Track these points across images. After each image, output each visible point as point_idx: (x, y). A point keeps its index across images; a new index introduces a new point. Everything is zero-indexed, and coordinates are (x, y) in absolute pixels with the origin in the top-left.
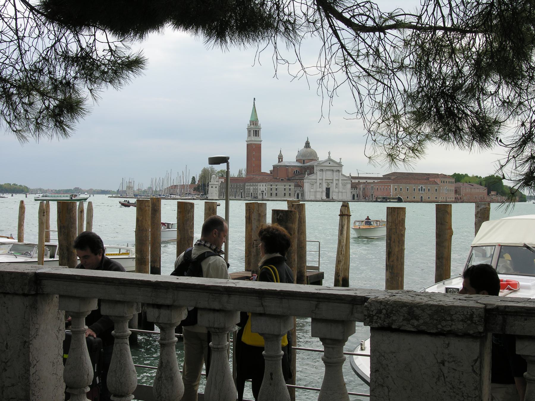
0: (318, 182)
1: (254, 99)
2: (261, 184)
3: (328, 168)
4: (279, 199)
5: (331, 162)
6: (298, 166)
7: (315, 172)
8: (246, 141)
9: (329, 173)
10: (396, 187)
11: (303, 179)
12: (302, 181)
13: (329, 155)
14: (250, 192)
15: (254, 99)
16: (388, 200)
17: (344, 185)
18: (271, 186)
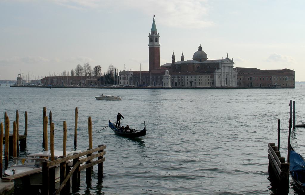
0: (223, 74)
1: (154, 16)
2: (189, 77)
3: (227, 65)
4: (204, 86)
5: (228, 61)
6: (199, 63)
9: (227, 68)
10: (275, 78)
11: (213, 73)
12: (212, 74)
13: (227, 56)
14: (174, 81)
15: (154, 16)
16: (277, 87)
17: (234, 77)
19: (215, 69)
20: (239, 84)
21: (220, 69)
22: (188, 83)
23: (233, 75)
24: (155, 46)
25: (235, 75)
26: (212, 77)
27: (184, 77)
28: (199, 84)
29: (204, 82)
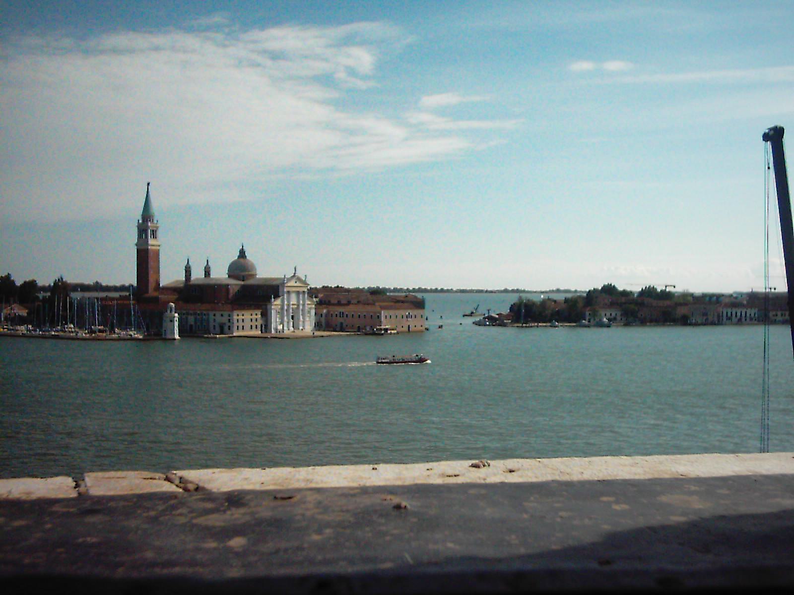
1: (148, 184)
2: (218, 314)
3: (294, 289)
7: (280, 294)
8: (136, 245)
11: (266, 305)
15: (148, 184)
18: (238, 315)
19: (271, 298)
20: (318, 326)
21: (279, 297)
22: (214, 326)
23: (306, 308)
24: (149, 247)
25: (311, 308)
26: (265, 315)
27: (208, 315)
28: (238, 329)
29: (247, 324)
